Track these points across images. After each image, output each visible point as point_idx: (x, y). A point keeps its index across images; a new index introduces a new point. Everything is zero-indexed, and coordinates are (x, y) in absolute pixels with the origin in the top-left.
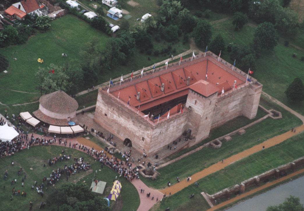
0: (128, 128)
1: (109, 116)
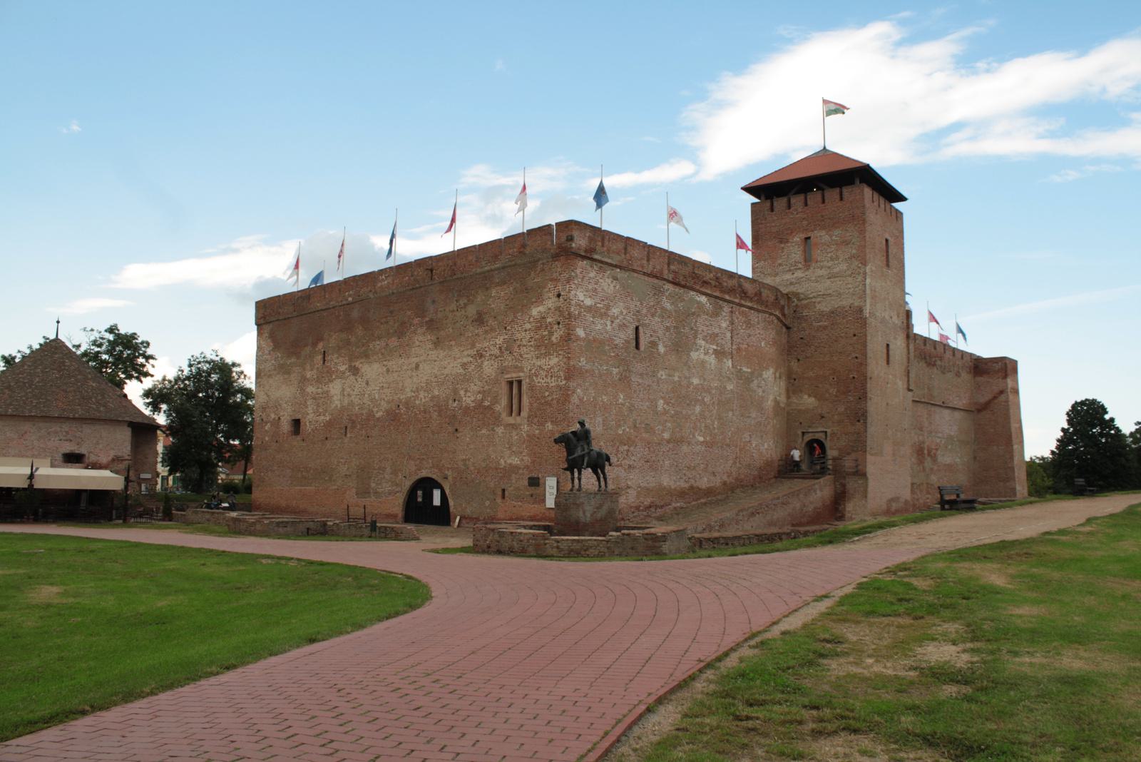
0: (407, 403)
1: (311, 419)
